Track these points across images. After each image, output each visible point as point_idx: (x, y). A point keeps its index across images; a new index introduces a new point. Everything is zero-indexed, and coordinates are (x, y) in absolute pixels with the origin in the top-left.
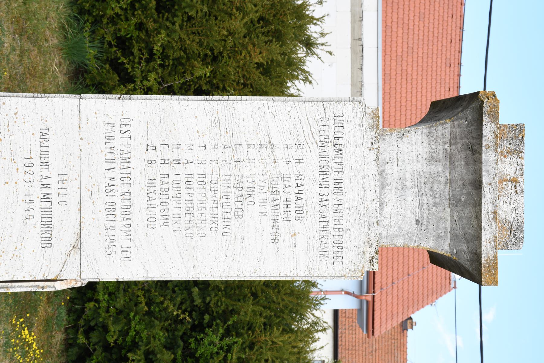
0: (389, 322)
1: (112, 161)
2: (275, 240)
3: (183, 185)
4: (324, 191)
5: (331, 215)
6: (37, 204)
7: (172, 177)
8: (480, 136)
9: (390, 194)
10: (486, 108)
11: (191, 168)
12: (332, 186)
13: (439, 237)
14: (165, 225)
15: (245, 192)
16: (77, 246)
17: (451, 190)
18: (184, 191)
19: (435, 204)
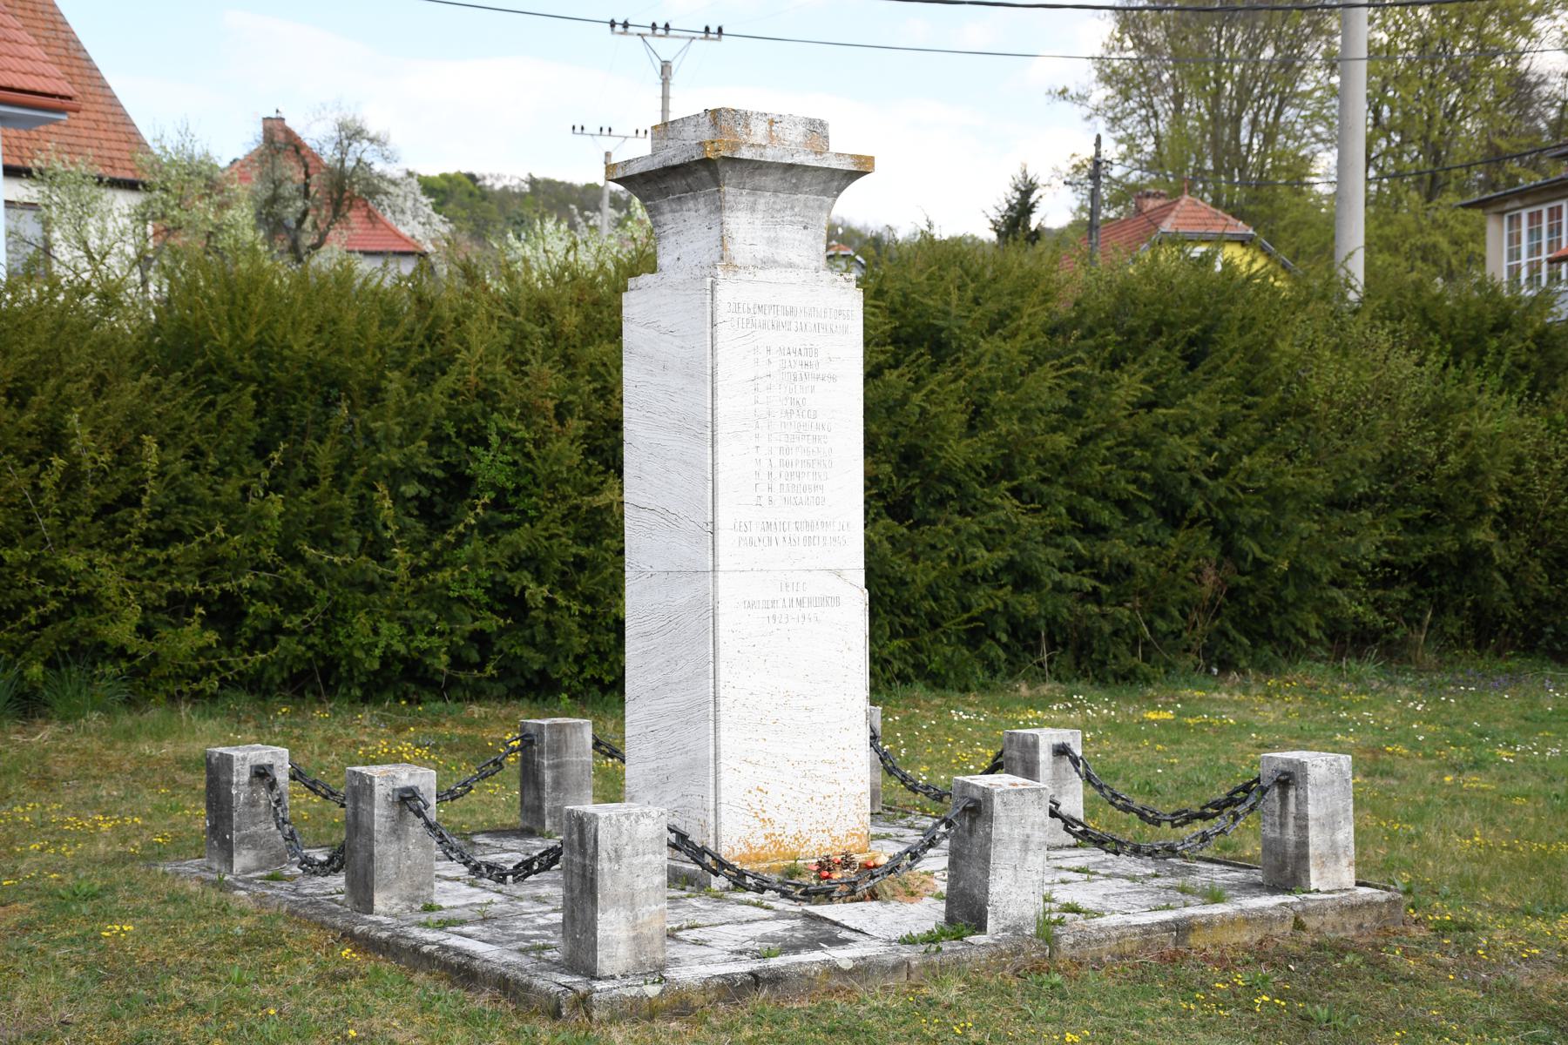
0: (26, 50)
1: (770, 540)
2: (833, 378)
3: (790, 470)
4: (793, 326)
5: (814, 320)
6: (806, 611)
7: (783, 481)
8: (750, 161)
9: (783, 255)
10: (728, 154)
11: (776, 462)
12: (788, 318)
13: (820, 208)
14: (822, 488)
15: (795, 408)
16: (838, 573)
17: (783, 191)
18: (794, 469)
19: (792, 208)
